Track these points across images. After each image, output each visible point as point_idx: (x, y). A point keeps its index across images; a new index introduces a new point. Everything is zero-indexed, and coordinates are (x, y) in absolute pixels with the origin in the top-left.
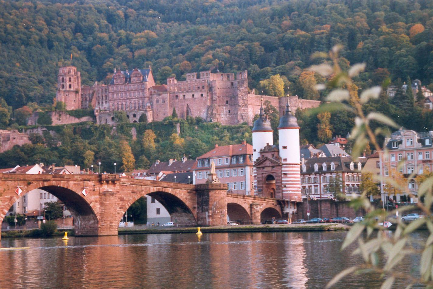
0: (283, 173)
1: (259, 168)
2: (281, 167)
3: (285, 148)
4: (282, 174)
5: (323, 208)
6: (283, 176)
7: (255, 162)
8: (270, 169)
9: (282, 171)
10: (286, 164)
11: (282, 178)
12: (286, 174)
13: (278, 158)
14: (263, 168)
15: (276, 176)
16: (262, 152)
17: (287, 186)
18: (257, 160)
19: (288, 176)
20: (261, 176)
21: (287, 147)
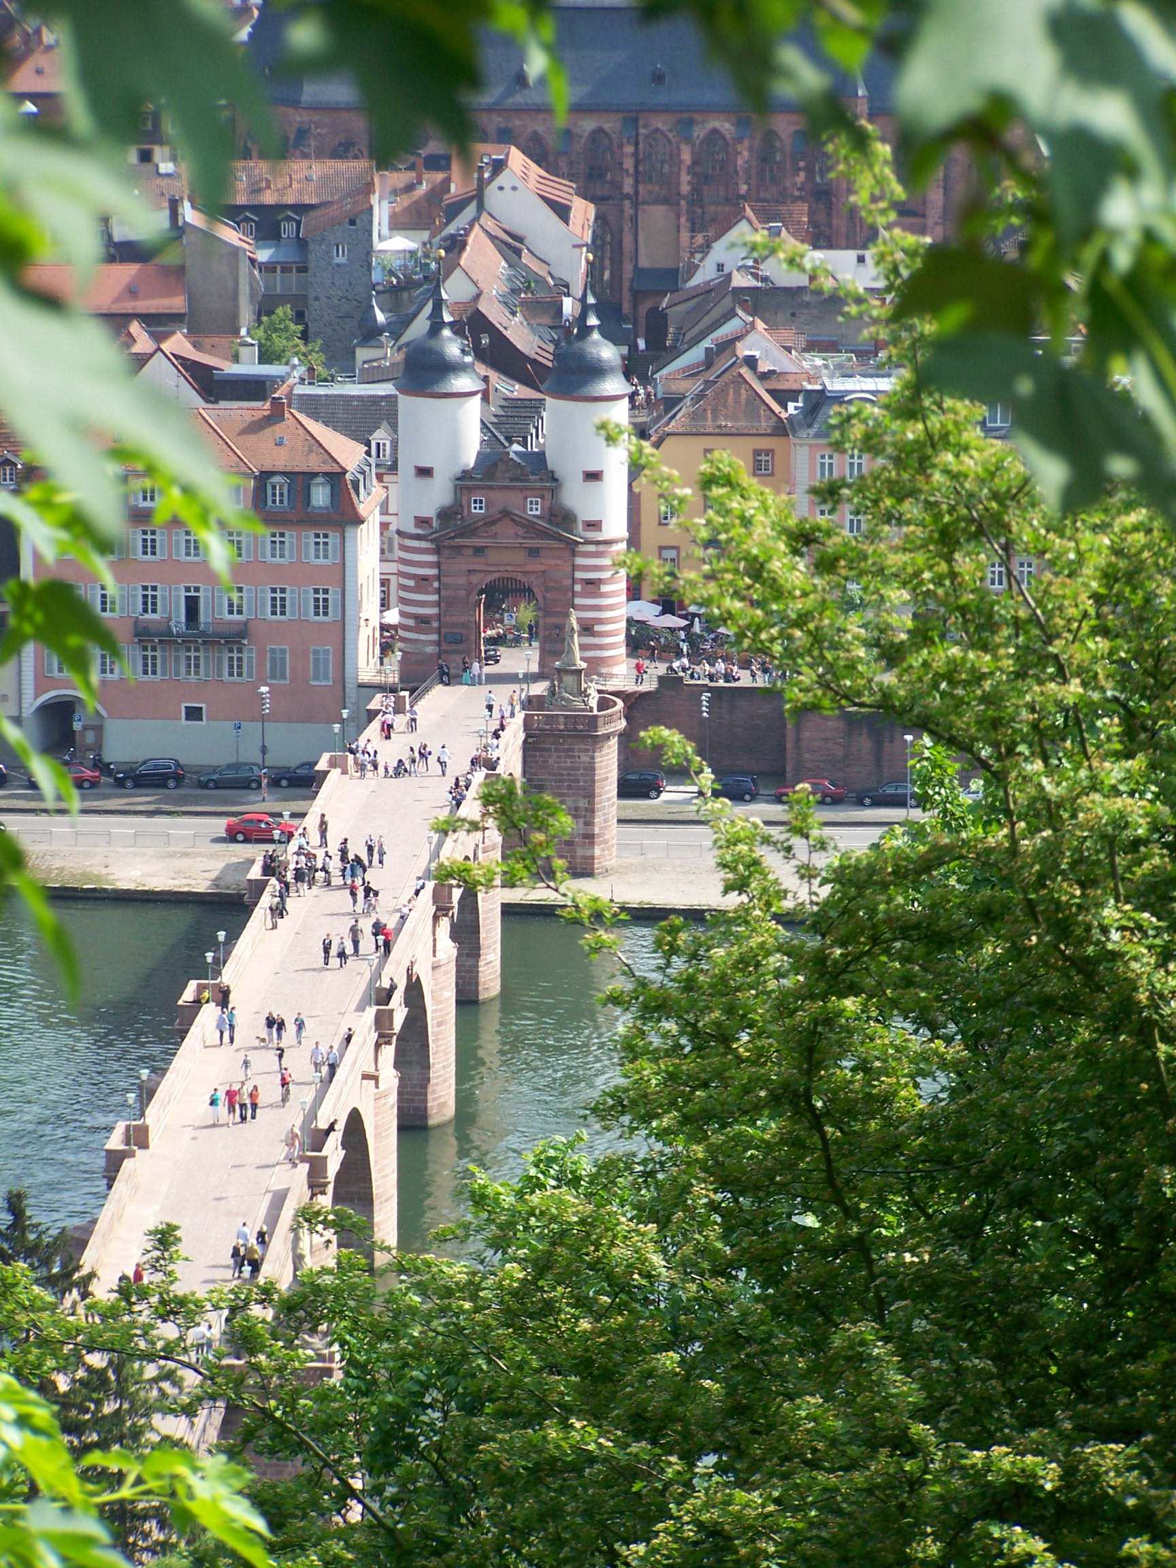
0: (579, 575)
1: (460, 548)
2: (574, 554)
3: (593, 476)
4: (574, 581)
5: (806, 735)
6: (578, 588)
7: (421, 522)
8: (520, 557)
9: (574, 568)
10: (598, 543)
11: (574, 594)
12: (590, 582)
13: (562, 518)
14: (479, 551)
15: (547, 589)
16: (465, 481)
17: (597, 628)
18: (445, 515)
19: (605, 588)
20: (462, 580)
21: (605, 476)
